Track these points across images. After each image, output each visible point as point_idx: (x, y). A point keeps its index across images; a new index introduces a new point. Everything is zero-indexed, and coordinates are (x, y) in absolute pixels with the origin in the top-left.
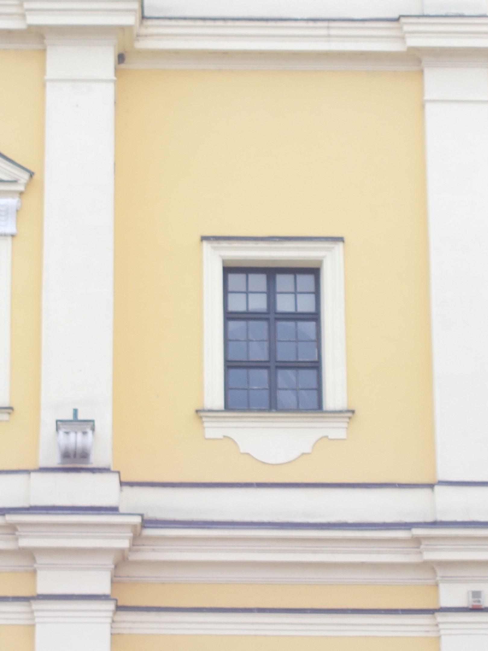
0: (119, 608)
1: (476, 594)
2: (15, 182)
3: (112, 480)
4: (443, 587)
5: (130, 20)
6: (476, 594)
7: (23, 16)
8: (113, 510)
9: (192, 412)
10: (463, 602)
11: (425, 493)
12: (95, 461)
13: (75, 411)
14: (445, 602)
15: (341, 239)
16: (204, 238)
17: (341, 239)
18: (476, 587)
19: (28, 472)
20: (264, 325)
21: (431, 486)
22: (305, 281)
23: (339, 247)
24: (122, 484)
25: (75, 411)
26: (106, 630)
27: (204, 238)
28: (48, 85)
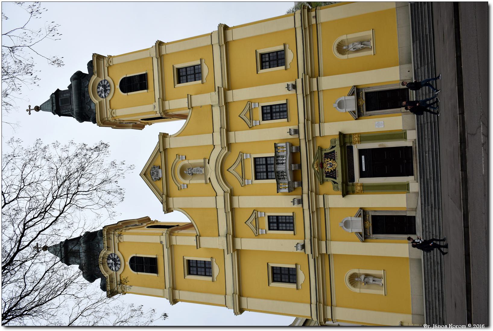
0: (319, 76)
1: (313, 17)
2: (250, 104)
3: (298, 80)
4: (312, 23)
5: (222, 88)
6: (313, 17)
7: (223, 106)
8: (302, 79)
9: (286, 71)
10: (315, 19)
11: (297, 29)
12: (294, 83)
13: (286, 88)
14: (315, 22)
15: (256, 51)
16: (257, 73)
17: (256, 51)
18: (312, 17)
19: (297, 94)
20: (271, 62)
21: (295, 28)
22: (263, 56)
23: (257, 51)
24: (298, 78)
25: (286, 88)
26: (323, 78)
27: (257, 73)
28: (234, 101)
